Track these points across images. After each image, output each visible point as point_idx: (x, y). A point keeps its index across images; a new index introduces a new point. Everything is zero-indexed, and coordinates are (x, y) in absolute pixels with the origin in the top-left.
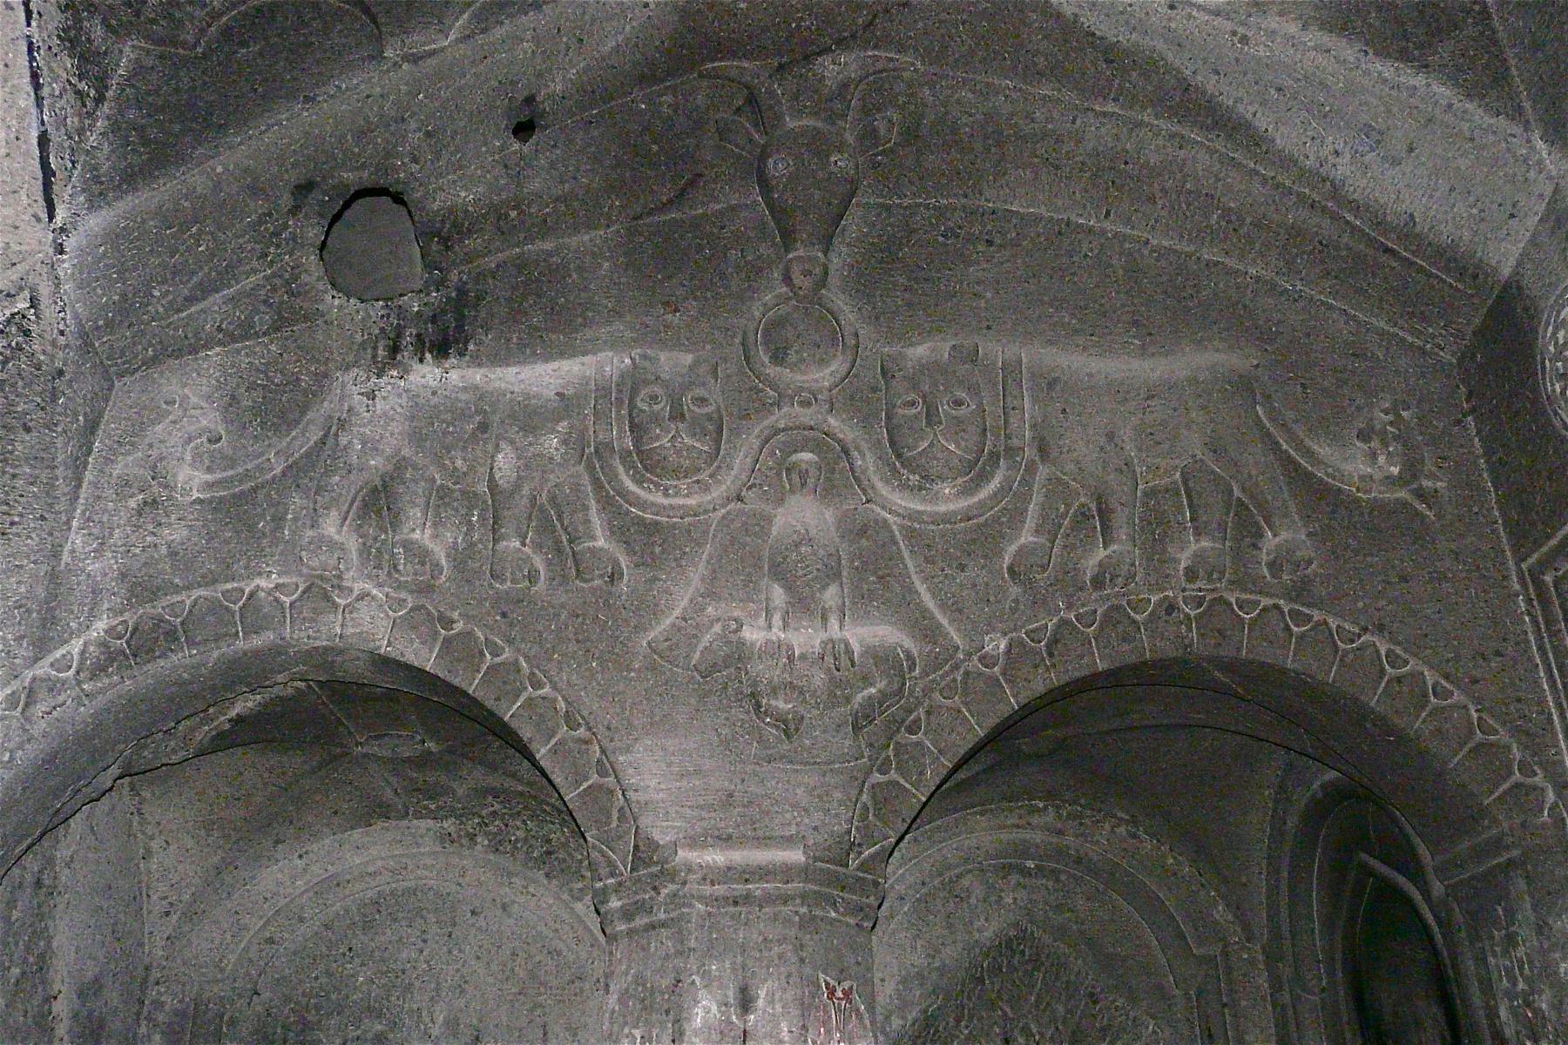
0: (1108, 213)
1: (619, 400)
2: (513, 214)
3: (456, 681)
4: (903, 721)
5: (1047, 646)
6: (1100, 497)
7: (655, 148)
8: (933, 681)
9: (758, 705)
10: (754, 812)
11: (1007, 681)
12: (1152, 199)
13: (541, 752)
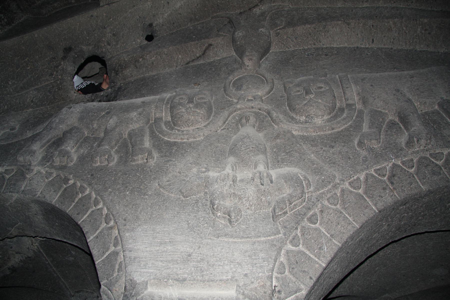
0: (373, 40)
1: (167, 103)
2: (141, 60)
3: (63, 208)
4: (305, 214)
5: (389, 179)
6: (399, 113)
7: (194, 37)
8: (323, 193)
9: (213, 204)
10: (204, 265)
11: (369, 197)
12: (390, 30)
13: (90, 238)
